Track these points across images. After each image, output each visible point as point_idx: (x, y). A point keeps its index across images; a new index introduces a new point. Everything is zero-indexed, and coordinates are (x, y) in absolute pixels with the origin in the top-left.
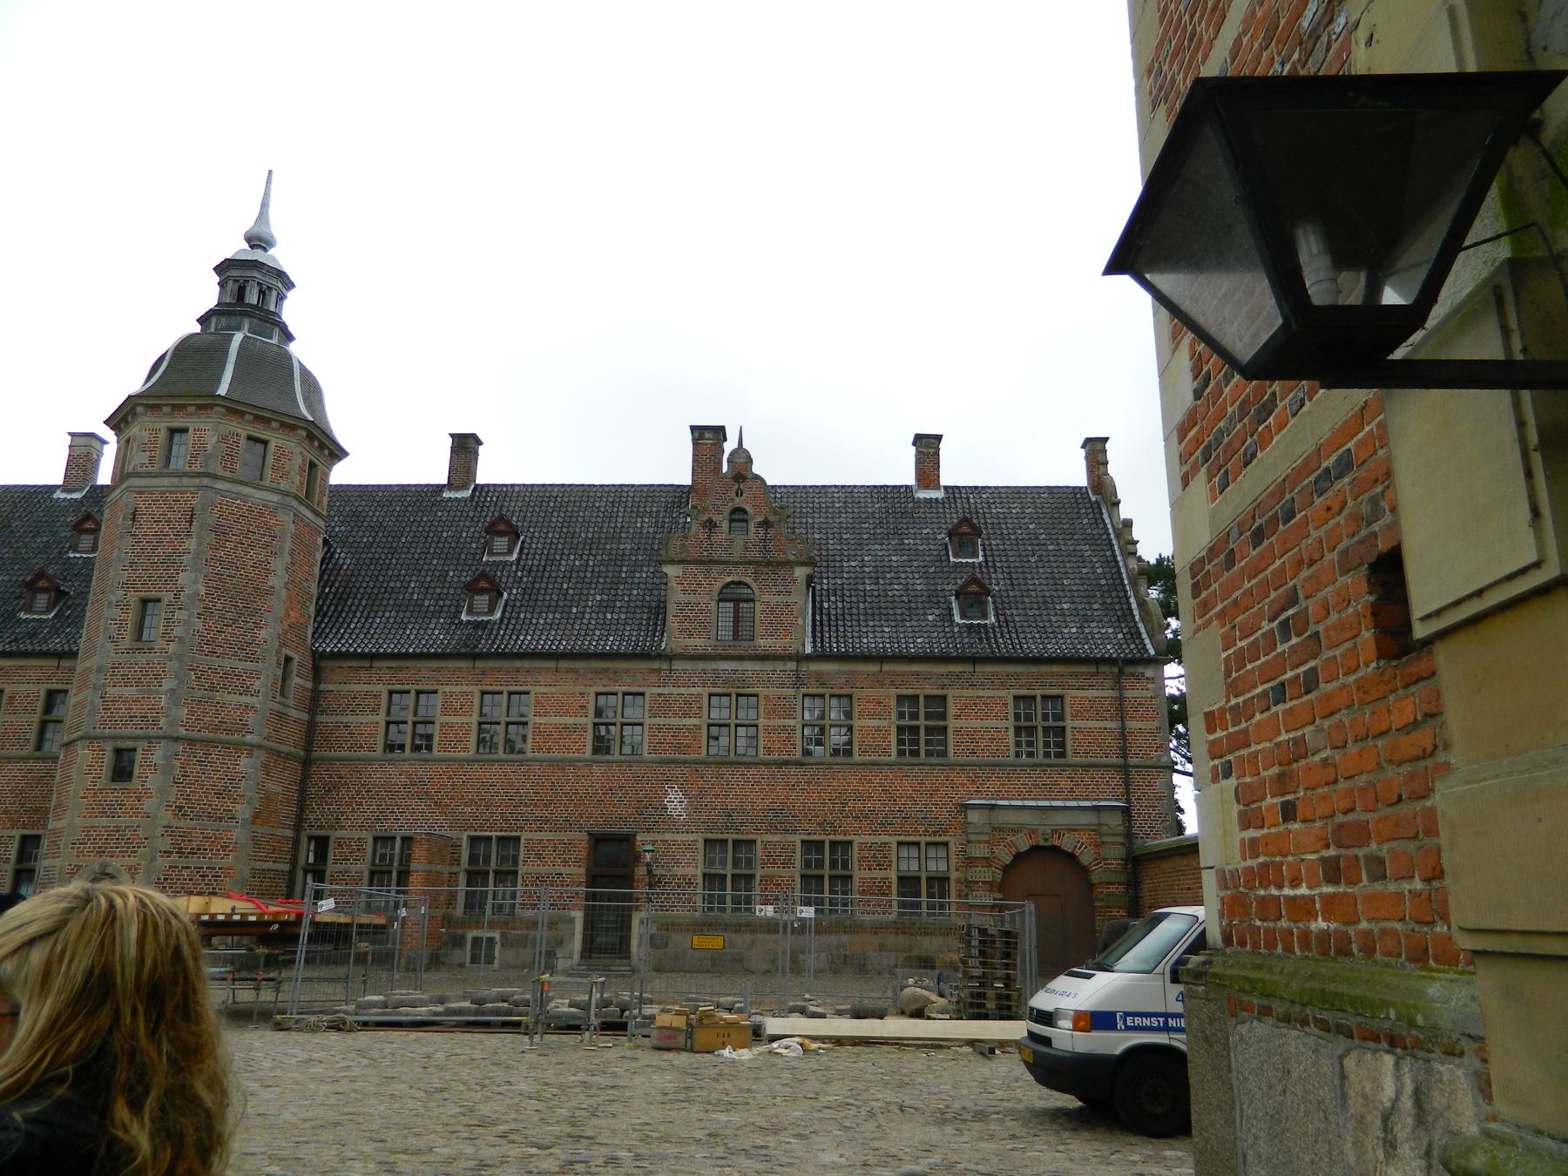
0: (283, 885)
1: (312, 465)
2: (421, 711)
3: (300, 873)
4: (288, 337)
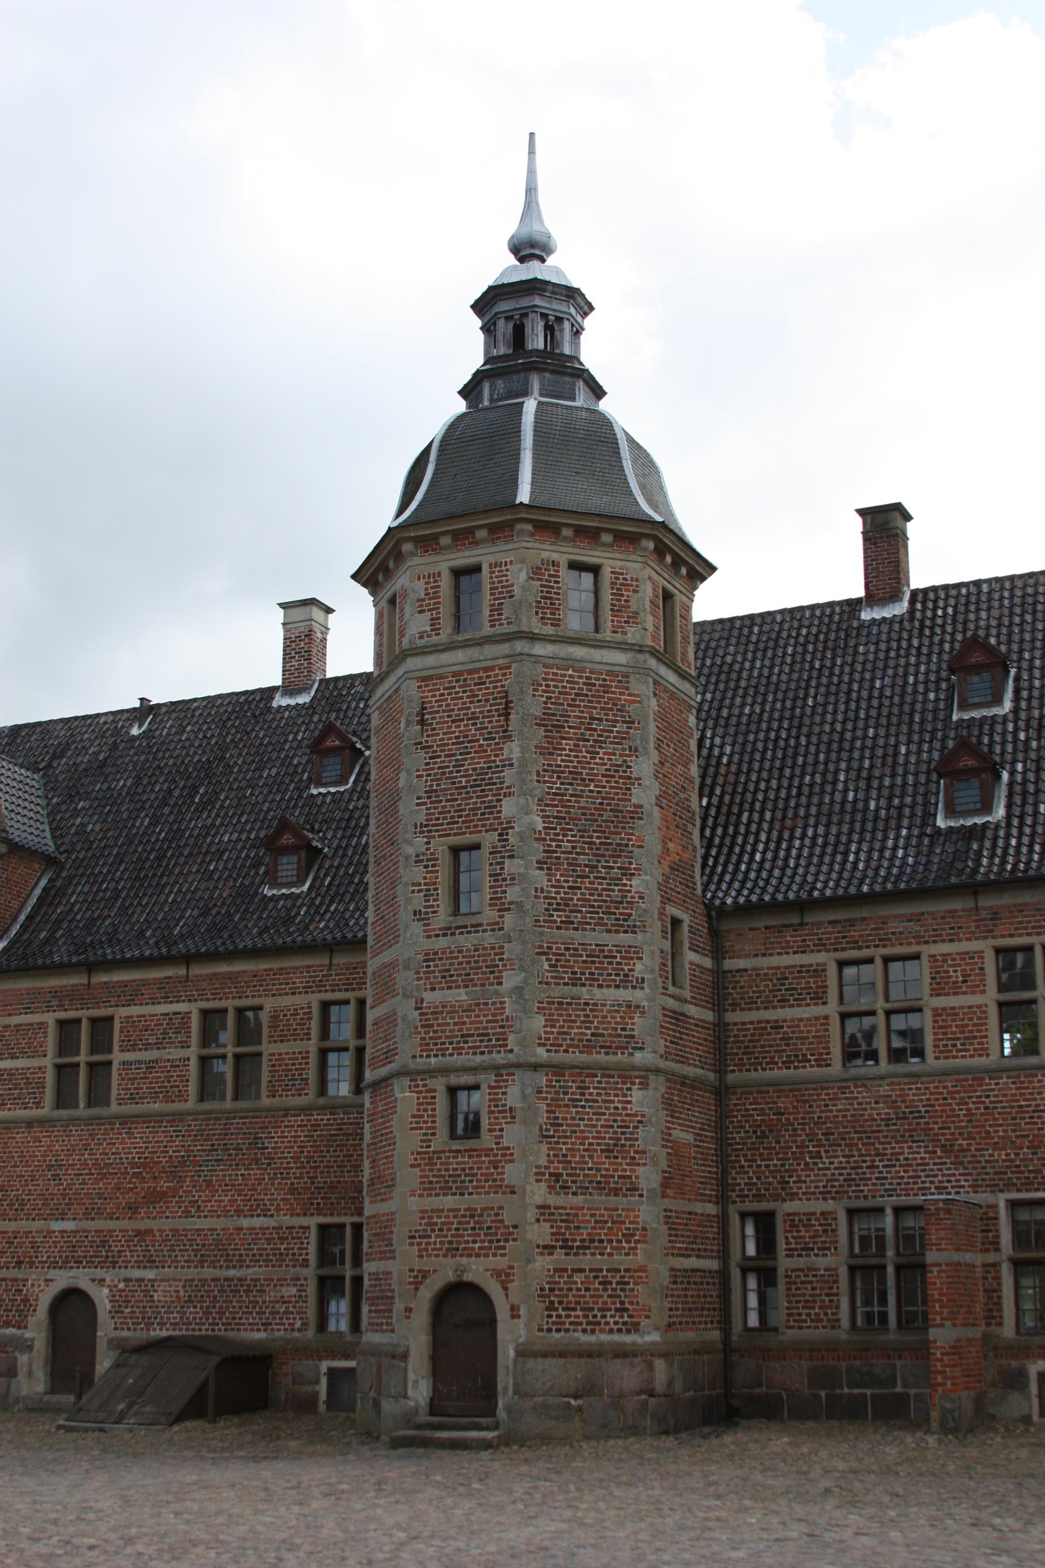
0: (714, 1294)
1: (667, 596)
2: (896, 993)
3: (736, 1274)
4: (598, 392)
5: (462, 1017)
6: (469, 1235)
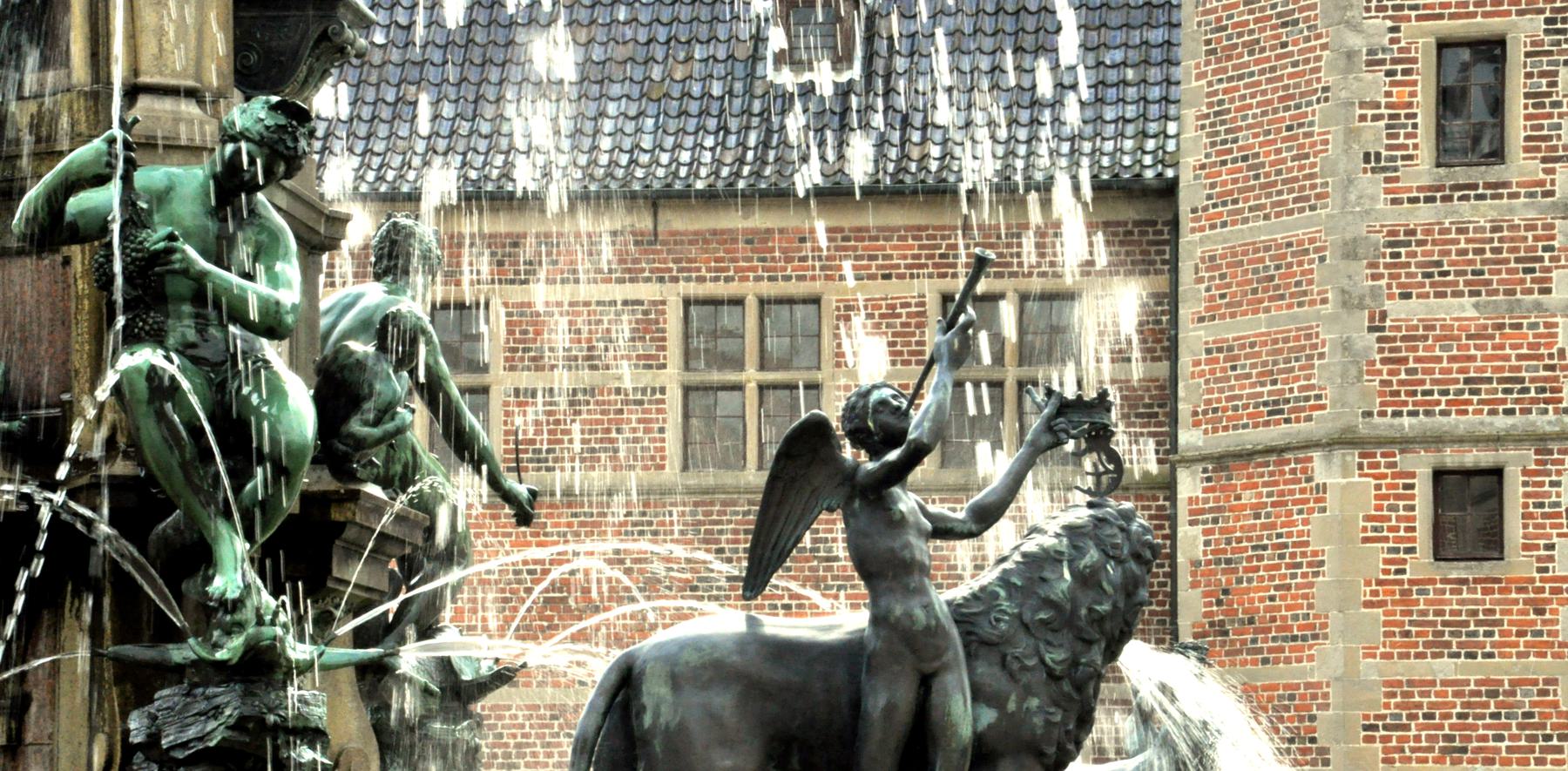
5: (1467, 347)
6: (1486, 727)
